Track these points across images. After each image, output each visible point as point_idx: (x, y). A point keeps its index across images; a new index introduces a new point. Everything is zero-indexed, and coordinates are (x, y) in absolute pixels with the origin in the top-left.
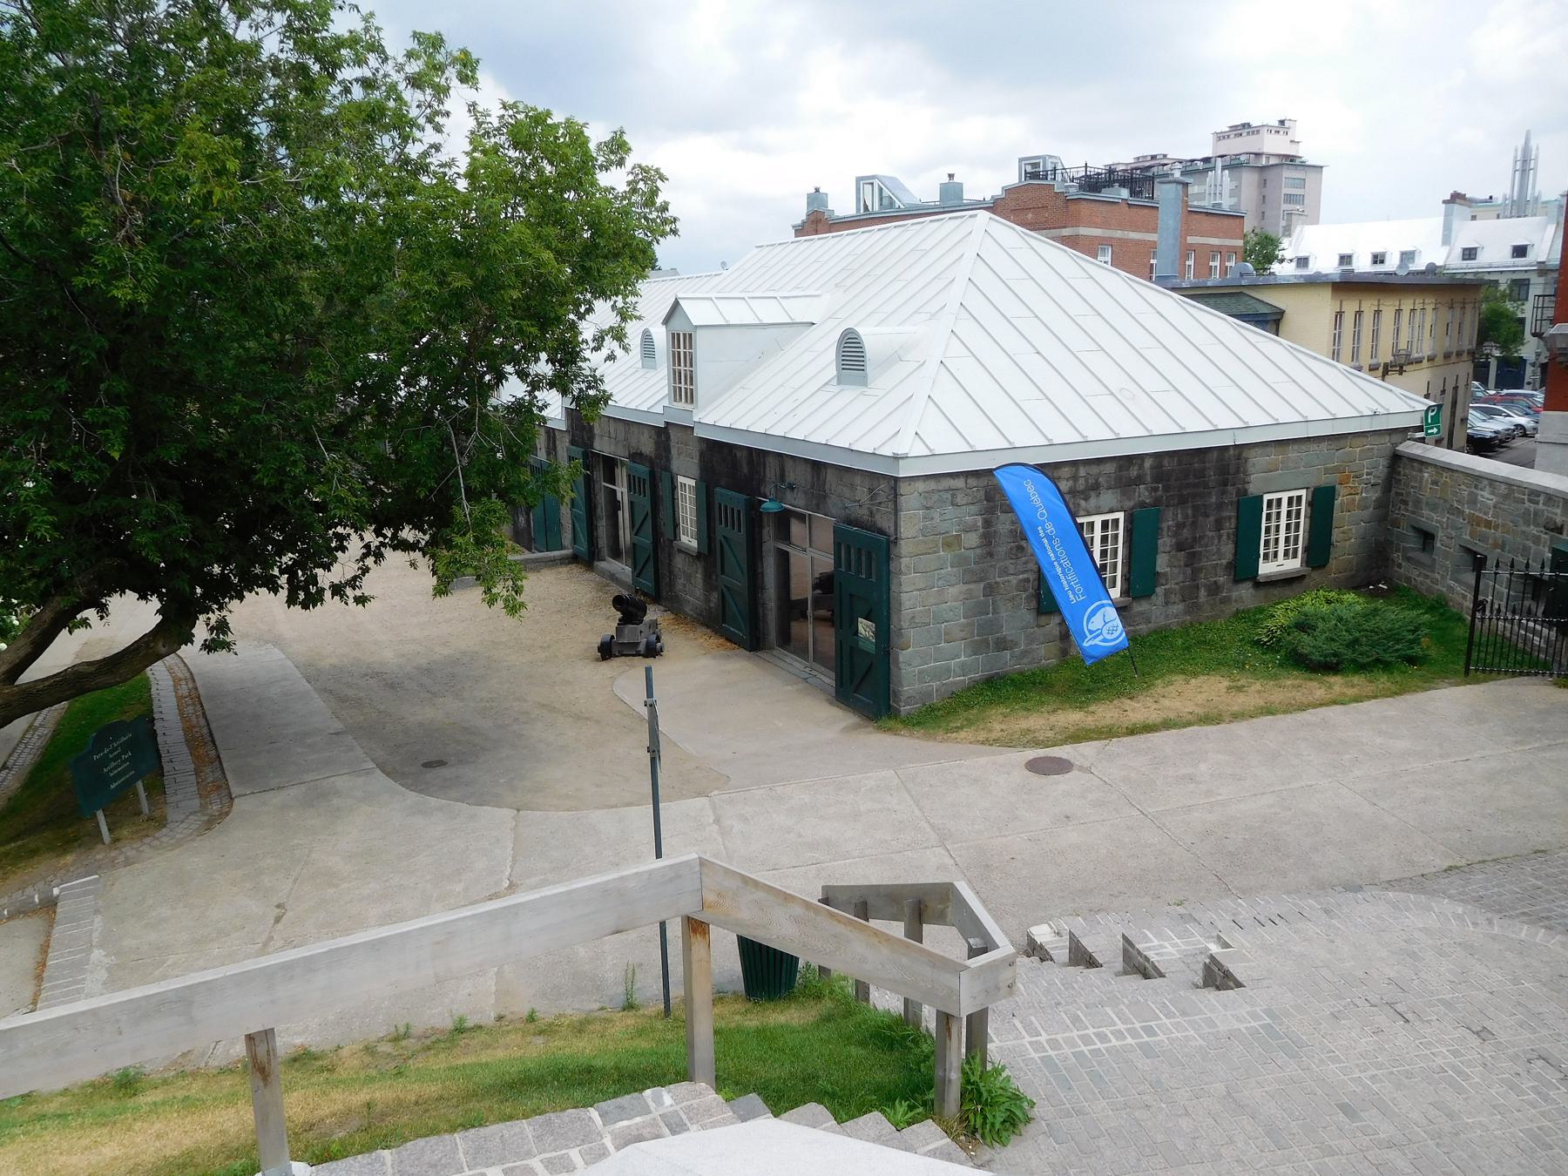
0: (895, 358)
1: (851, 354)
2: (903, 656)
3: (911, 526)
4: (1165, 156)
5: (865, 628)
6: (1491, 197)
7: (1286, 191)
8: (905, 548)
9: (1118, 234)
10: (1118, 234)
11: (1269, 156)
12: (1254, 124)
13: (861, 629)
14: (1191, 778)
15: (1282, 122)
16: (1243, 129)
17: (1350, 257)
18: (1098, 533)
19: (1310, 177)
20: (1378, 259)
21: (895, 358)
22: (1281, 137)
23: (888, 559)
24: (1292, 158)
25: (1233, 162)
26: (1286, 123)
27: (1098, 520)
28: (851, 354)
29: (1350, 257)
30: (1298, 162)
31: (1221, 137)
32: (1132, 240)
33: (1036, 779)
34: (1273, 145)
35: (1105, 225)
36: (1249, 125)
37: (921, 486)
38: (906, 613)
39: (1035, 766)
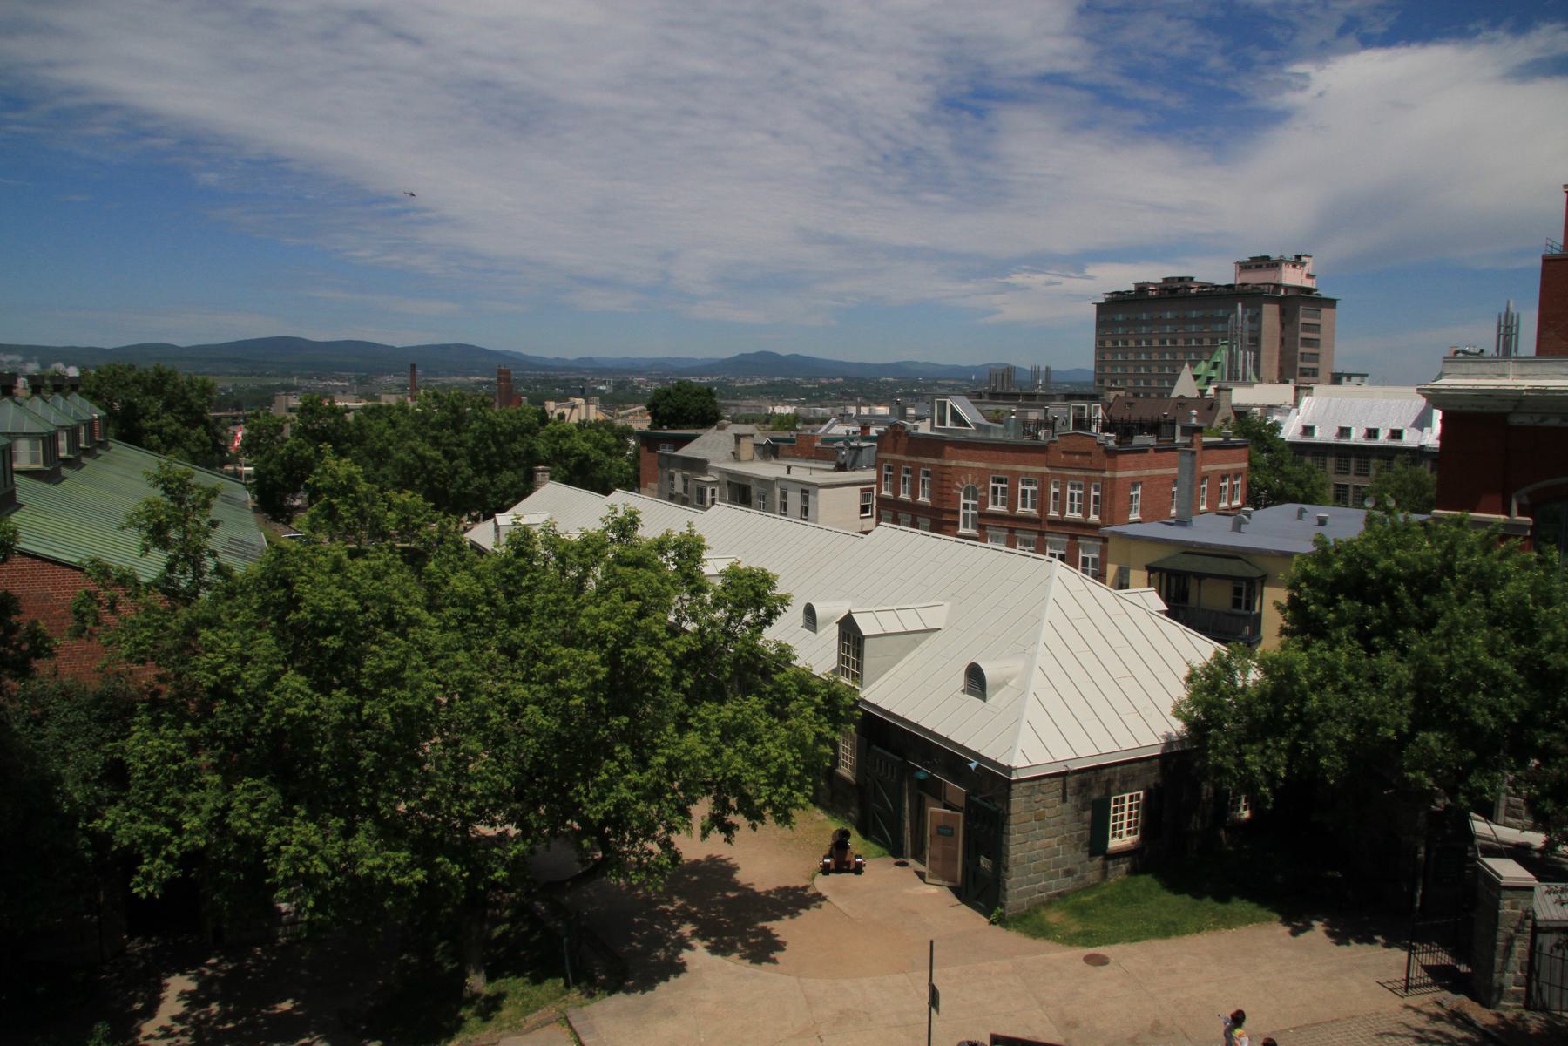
0: (1002, 684)
1: (976, 680)
2: (1009, 883)
3: (1018, 803)
4: (1192, 279)
5: (984, 862)
6: (1482, 351)
7: (1302, 320)
8: (1013, 819)
9: (1147, 472)
10: (1147, 472)
11: (1287, 288)
12: (1275, 256)
13: (982, 862)
14: (1173, 971)
15: (1298, 257)
16: (1262, 263)
17: (1348, 430)
18: (1127, 804)
19: (1325, 312)
20: (1373, 433)
21: (1002, 684)
22: (1298, 271)
23: (1003, 824)
24: (1309, 290)
25: (1255, 291)
26: (1304, 259)
27: (1127, 796)
28: (976, 680)
29: (1348, 430)
30: (1313, 295)
31: (1244, 267)
32: (1159, 475)
33: (1090, 968)
34: (1291, 277)
35: (1137, 466)
36: (1267, 258)
37: (1023, 784)
38: (1012, 857)
39: (1090, 959)
